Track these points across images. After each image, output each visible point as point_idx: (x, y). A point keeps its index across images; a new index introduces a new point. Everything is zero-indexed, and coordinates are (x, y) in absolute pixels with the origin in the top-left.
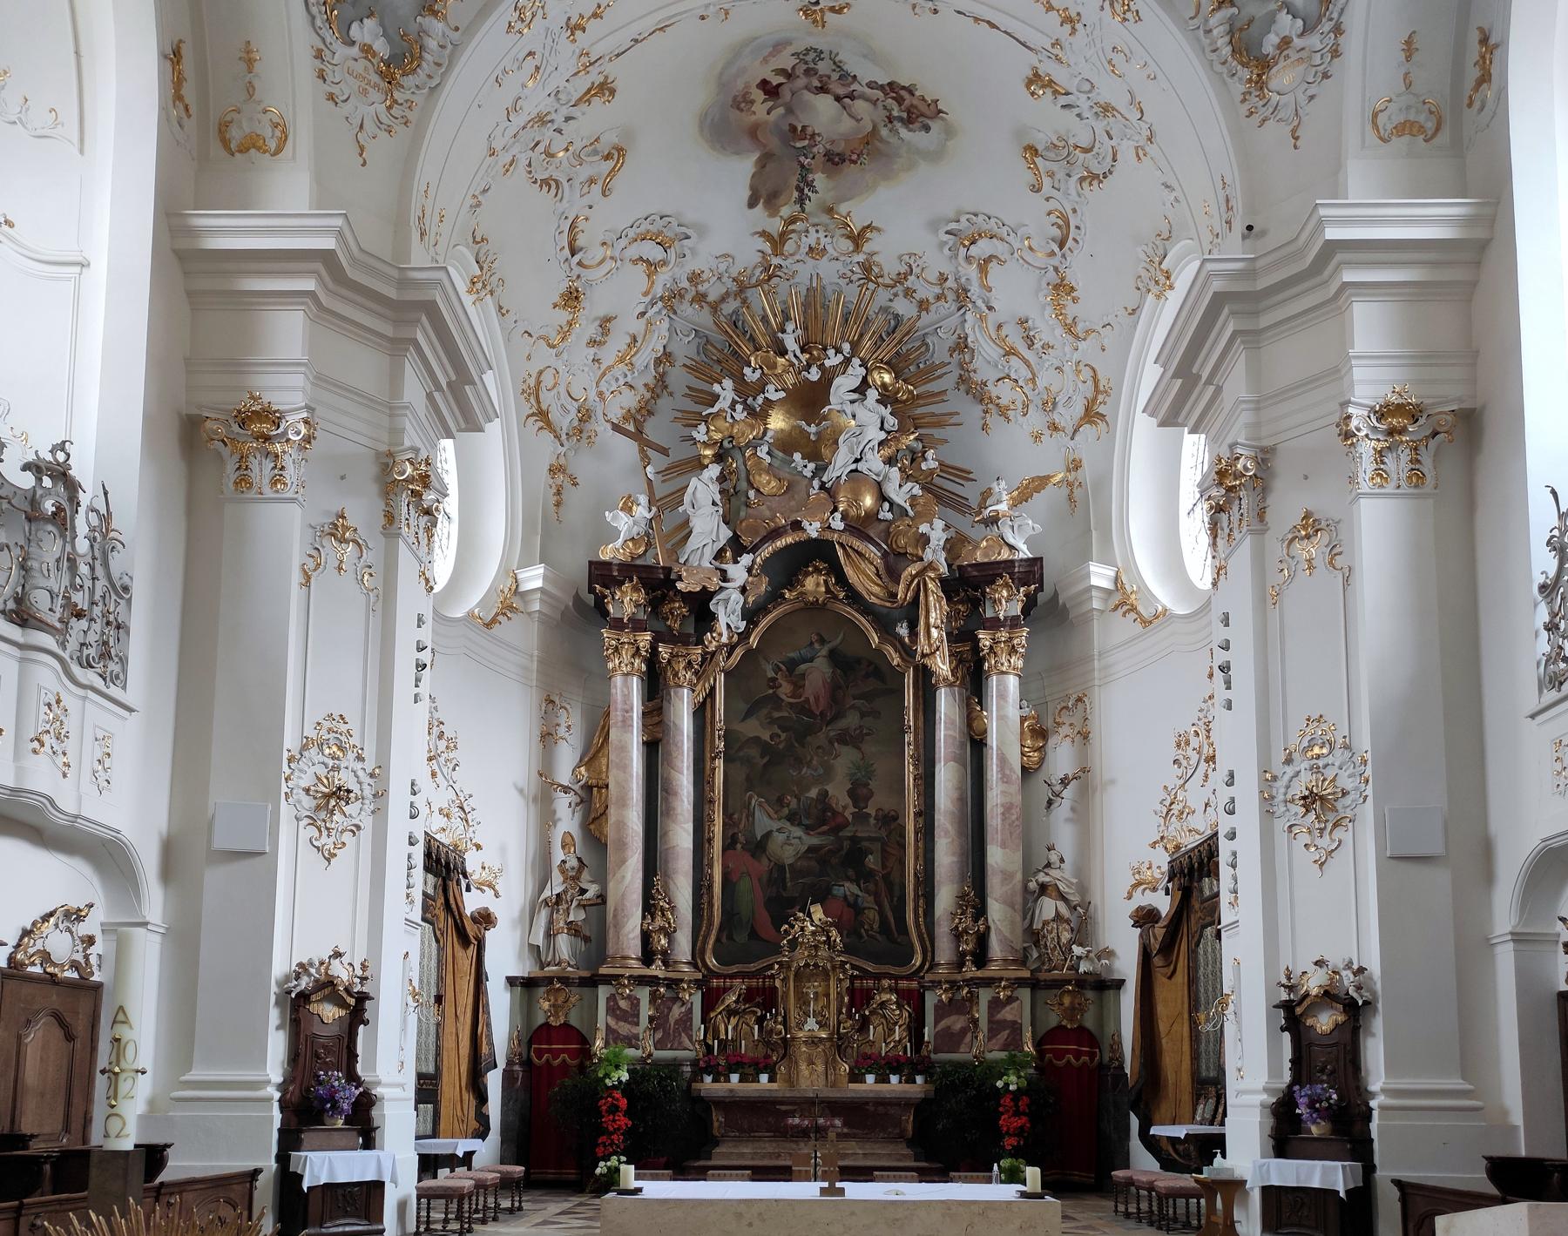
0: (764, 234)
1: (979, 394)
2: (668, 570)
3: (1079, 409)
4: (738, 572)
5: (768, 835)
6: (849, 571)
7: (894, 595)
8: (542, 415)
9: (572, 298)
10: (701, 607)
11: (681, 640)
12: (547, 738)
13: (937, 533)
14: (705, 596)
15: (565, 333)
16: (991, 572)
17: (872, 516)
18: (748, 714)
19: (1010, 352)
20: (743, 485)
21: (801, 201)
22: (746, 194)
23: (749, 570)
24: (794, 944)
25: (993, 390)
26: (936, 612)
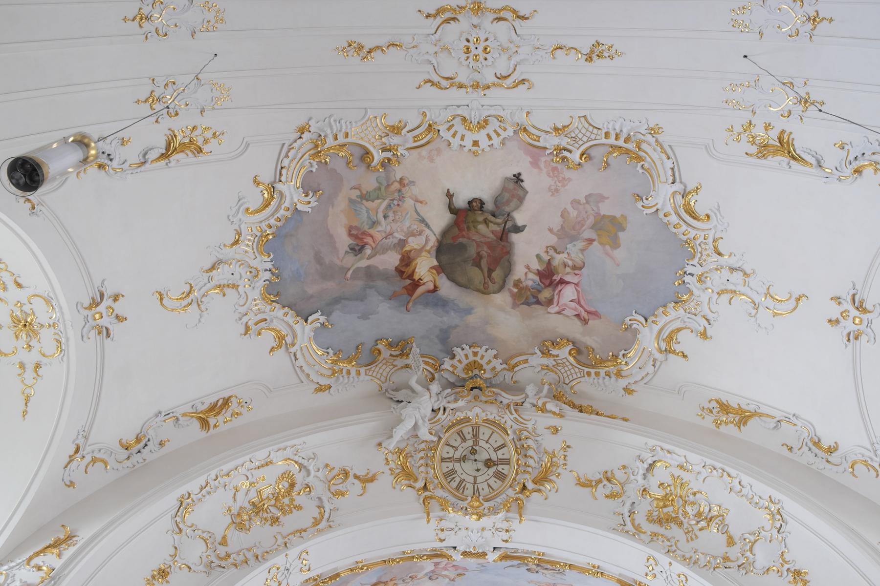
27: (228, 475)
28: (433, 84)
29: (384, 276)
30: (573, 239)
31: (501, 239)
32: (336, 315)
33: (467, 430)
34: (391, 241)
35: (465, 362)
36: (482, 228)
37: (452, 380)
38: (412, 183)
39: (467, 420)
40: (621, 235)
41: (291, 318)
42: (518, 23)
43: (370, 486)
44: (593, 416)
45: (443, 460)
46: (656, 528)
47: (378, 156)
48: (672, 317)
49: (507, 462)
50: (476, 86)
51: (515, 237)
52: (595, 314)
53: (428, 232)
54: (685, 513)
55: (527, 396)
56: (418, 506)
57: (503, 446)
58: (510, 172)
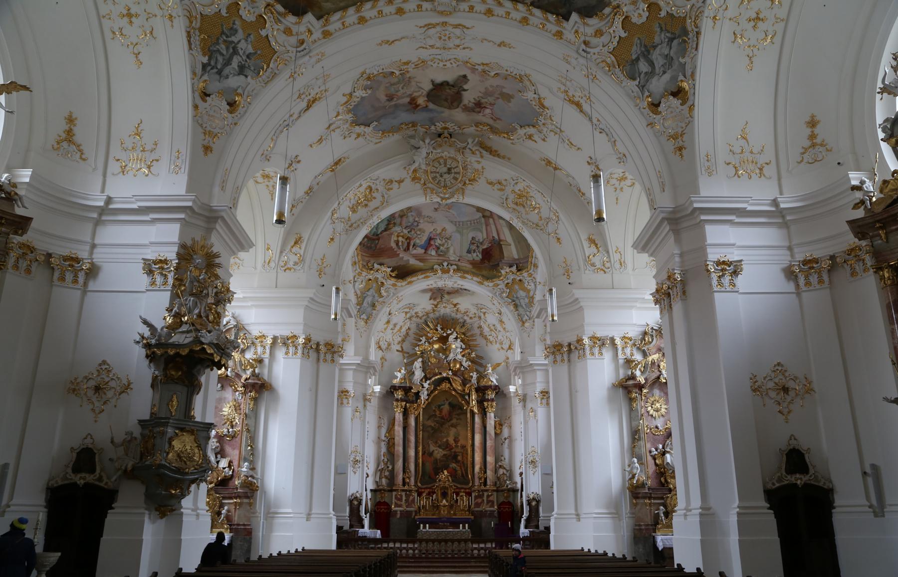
0: (433, 304)
1: (486, 339)
2: (409, 387)
3: (508, 346)
4: (426, 385)
5: (433, 451)
6: (453, 384)
7: (464, 390)
8: (380, 347)
9: (388, 322)
10: (417, 395)
11: (412, 402)
12: (379, 427)
13: (475, 375)
14: (419, 392)
15: (385, 329)
16: (487, 388)
17: (459, 369)
18: (428, 419)
19: (491, 330)
20: (427, 361)
21: (442, 299)
22: (429, 298)
23: (429, 384)
24: (440, 481)
25: (489, 337)
26: (474, 396)
27: (346, 196)
28: (423, 48)
29: (403, 105)
30: (490, 96)
31: (457, 93)
32: (382, 121)
33: (442, 161)
34: (406, 95)
35: (441, 127)
36: (448, 91)
37: (435, 132)
38: (415, 77)
39: (442, 157)
40: (512, 100)
41: (362, 127)
42: (465, 30)
43: (402, 184)
44: (496, 158)
45: (431, 172)
46: (515, 206)
47: (397, 73)
48: (531, 130)
49: (459, 173)
50: (444, 48)
51: (463, 93)
52: (499, 119)
53: (422, 90)
54: (526, 203)
55: (468, 143)
56: (422, 191)
57: (457, 167)
58: (462, 73)
